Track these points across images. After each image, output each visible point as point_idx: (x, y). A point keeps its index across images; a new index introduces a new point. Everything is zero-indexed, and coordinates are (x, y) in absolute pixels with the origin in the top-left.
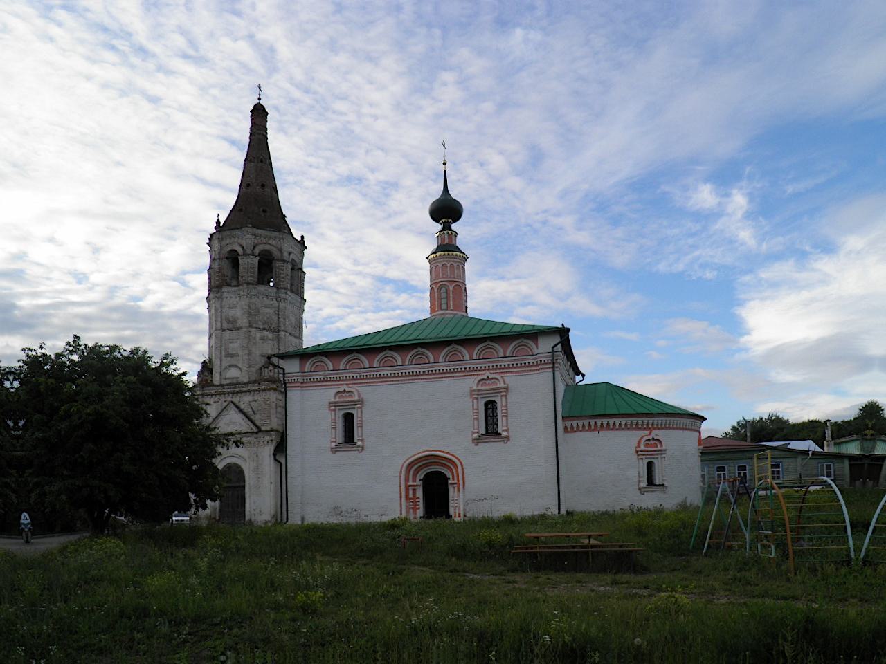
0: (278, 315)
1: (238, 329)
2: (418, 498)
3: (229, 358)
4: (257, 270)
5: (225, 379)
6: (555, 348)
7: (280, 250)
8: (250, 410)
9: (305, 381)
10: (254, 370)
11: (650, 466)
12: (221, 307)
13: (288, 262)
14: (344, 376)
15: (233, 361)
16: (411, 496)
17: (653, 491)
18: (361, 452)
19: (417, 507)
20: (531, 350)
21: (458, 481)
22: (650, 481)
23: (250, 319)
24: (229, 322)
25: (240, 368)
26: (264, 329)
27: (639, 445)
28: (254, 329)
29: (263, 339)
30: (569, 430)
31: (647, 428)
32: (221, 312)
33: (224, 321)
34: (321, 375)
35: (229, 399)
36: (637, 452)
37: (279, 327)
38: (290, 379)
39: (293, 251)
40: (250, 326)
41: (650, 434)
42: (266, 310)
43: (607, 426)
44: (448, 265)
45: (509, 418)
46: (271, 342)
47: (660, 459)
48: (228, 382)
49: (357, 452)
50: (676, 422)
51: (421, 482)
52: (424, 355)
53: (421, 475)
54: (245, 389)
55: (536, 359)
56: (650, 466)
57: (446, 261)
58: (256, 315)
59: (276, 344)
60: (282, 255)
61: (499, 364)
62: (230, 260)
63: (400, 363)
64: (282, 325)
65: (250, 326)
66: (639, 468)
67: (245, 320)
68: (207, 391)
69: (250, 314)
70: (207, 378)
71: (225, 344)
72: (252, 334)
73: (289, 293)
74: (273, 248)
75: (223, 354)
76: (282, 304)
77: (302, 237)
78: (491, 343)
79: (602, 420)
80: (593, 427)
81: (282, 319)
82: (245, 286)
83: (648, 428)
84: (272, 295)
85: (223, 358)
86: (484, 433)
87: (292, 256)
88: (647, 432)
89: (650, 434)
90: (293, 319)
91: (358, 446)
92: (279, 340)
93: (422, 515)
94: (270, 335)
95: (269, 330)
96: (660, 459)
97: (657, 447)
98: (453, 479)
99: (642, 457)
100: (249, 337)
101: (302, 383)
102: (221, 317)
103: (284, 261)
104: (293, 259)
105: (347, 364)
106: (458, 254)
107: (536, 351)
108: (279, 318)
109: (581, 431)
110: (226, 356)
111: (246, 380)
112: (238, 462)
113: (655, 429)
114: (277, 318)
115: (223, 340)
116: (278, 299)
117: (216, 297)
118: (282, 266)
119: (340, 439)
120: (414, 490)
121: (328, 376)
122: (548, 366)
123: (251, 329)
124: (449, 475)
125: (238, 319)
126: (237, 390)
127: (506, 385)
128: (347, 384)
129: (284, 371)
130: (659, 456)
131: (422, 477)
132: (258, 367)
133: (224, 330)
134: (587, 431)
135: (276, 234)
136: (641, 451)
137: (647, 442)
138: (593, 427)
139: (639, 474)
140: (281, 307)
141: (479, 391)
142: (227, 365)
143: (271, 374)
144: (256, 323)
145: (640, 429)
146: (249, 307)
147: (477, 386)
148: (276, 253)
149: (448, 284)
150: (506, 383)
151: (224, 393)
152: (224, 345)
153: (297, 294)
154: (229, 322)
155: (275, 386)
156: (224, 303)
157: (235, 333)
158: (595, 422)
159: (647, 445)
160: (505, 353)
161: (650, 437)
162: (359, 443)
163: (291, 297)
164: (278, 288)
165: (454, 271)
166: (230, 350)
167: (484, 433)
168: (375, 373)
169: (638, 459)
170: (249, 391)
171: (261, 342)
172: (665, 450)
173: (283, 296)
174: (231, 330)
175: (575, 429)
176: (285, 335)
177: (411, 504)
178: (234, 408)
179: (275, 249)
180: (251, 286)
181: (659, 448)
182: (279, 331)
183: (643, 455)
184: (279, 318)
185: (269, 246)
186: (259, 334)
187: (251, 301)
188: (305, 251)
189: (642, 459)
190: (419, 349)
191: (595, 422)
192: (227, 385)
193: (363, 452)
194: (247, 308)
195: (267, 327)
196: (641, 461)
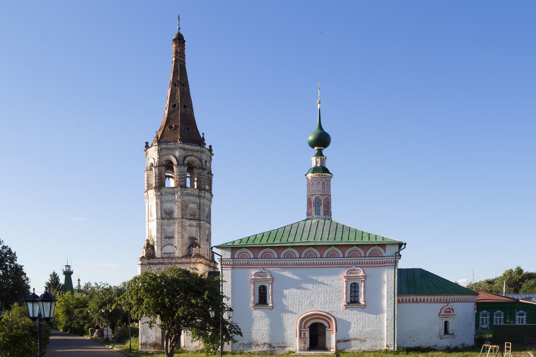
1: (174, 219)
2: (306, 338)
3: (167, 240)
5: (164, 254)
6: (396, 254)
7: (201, 160)
9: (235, 264)
10: (185, 248)
11: (446, 323)
12: (161, 202)
14: (261, 262)
16: (303, 336)
17: (447, 338)
18: (271, 310)
19: (306, 343)
20: (381, 254)
21: (333, 329)
22: (446, 332)
23: (183, 213)
24: (167, 213)
26: (191, 219)
27: (441, 312)
28: (185, 220)
29: (190, 226)
30: (401, 302)
31: (446, 302)
32: (161, 206)
34: (245, 261)
36: (439, 315)
37: (200, 218)
38: (225, 262)
40: (183, 218)
41: (447, 306)
42: (192, 206)
43: (423, 300)
44: (321, 183)
45: (366, 294)
46: (195, 229)
47: (452, 319)
48: (166, 256)
49: (269, 309)
50: (462, 298)
51: (309, 328)
52: (313, 252)
53: (309, 324)
54: (179, 261)
55: (384, 259)
56: (446, 323)
57: (320, 180)
58: (186, 210)
59: (198, 230)
60: (202, 164)
61: (361, 261)
62: (165, 166)
63: (298, 256)
64: (202, 216)
65: (183, 218)
66: (440, 325)
67: (180, 214)
68: (151, 261)
69: (182, 209)
70: (150, 252)
71: (164, 229)
72: (183, 224)
74: (196, 159)
75: (163, 236)
76: (202, 201)
77: (210, 146)
78: (357, 248)
79: (421, 297)
80: (415, 301)
81: (202, 212)
82: (179, 188)
83: (447, 302)
84: (196, 195)
85: (163, 239)
86: (350, 302)
88: (446, 304)
89: (447, 306)
90: (207, 209)
91: (269, 307)
92: (200, 227)
93: (308, 347)
94: (194, 223)
95: (194, 219)
96: (452, 319)
97: (451, 313)
98: (330, 328)
99: (442, 318)
100: (183, 226)
101: (232, 265)
102: (161, 210)
105: (263, 255)
106: (330, 175)
107: (384, 254)
109: (408, 303)
111: (180, 255)
113: (451, 302)
114: (198, 211)
116: (199, 197)
117: (157, 194)
119: (257, 301)
120: (304, 334)
121: (250, 262)
122: (392, 264)
124: (326, 324)
126: (174, 261)
127: (364, 275)
128: (262, 268)
129: (221, 257)
130: (452, 318)
131: (309, 326)
132: (187, 246)
134: (411, 303)
135: (198, 148)
136: (442, 315)
137: (446, 310)
138: (415, 301)
139: (440, 328)
140: (201, 203)
141: (348, 277)
143: (198, 252)
144: (186, 215)
145: (443, 303)
147: (347, 274)
148: (197, 162)
149: (321, 197)
150: (365, 273)
151: (164, 264)
152: (163, 230)
154: (167, 213)
155: (201, 261)
156: (163, 200)
157: (171, 221)
158: (417, 298)
159: (445, 312)
160: (365, 254)
161: (447, 307)
162: (271, 305)
163: (207, 195)
164: (200, 190)
165: (325, 188)
166: (167, 234)
167: (350, 302)
168: (281, 262)
169: (440, 320)
171: (189, 228)
172: (456, 315)
173: (202, 194)
174: (168, 219)
175: (404, 301)
176: (204, 224)
177: (303, 341)
179: (198, 160)
180: (183, 189)
181: (452, 313)
183: (443, 317)
184: (200, 211)
185: (194, 158)
186: (188, 222)
187: (183, 199)
189: (442, 319)
190: (311, 248)
191: (417, 298)
192: (166, 258)
193: (273, 310)
194: (180, 204)
195: (192, 217)
196: (441, 321)
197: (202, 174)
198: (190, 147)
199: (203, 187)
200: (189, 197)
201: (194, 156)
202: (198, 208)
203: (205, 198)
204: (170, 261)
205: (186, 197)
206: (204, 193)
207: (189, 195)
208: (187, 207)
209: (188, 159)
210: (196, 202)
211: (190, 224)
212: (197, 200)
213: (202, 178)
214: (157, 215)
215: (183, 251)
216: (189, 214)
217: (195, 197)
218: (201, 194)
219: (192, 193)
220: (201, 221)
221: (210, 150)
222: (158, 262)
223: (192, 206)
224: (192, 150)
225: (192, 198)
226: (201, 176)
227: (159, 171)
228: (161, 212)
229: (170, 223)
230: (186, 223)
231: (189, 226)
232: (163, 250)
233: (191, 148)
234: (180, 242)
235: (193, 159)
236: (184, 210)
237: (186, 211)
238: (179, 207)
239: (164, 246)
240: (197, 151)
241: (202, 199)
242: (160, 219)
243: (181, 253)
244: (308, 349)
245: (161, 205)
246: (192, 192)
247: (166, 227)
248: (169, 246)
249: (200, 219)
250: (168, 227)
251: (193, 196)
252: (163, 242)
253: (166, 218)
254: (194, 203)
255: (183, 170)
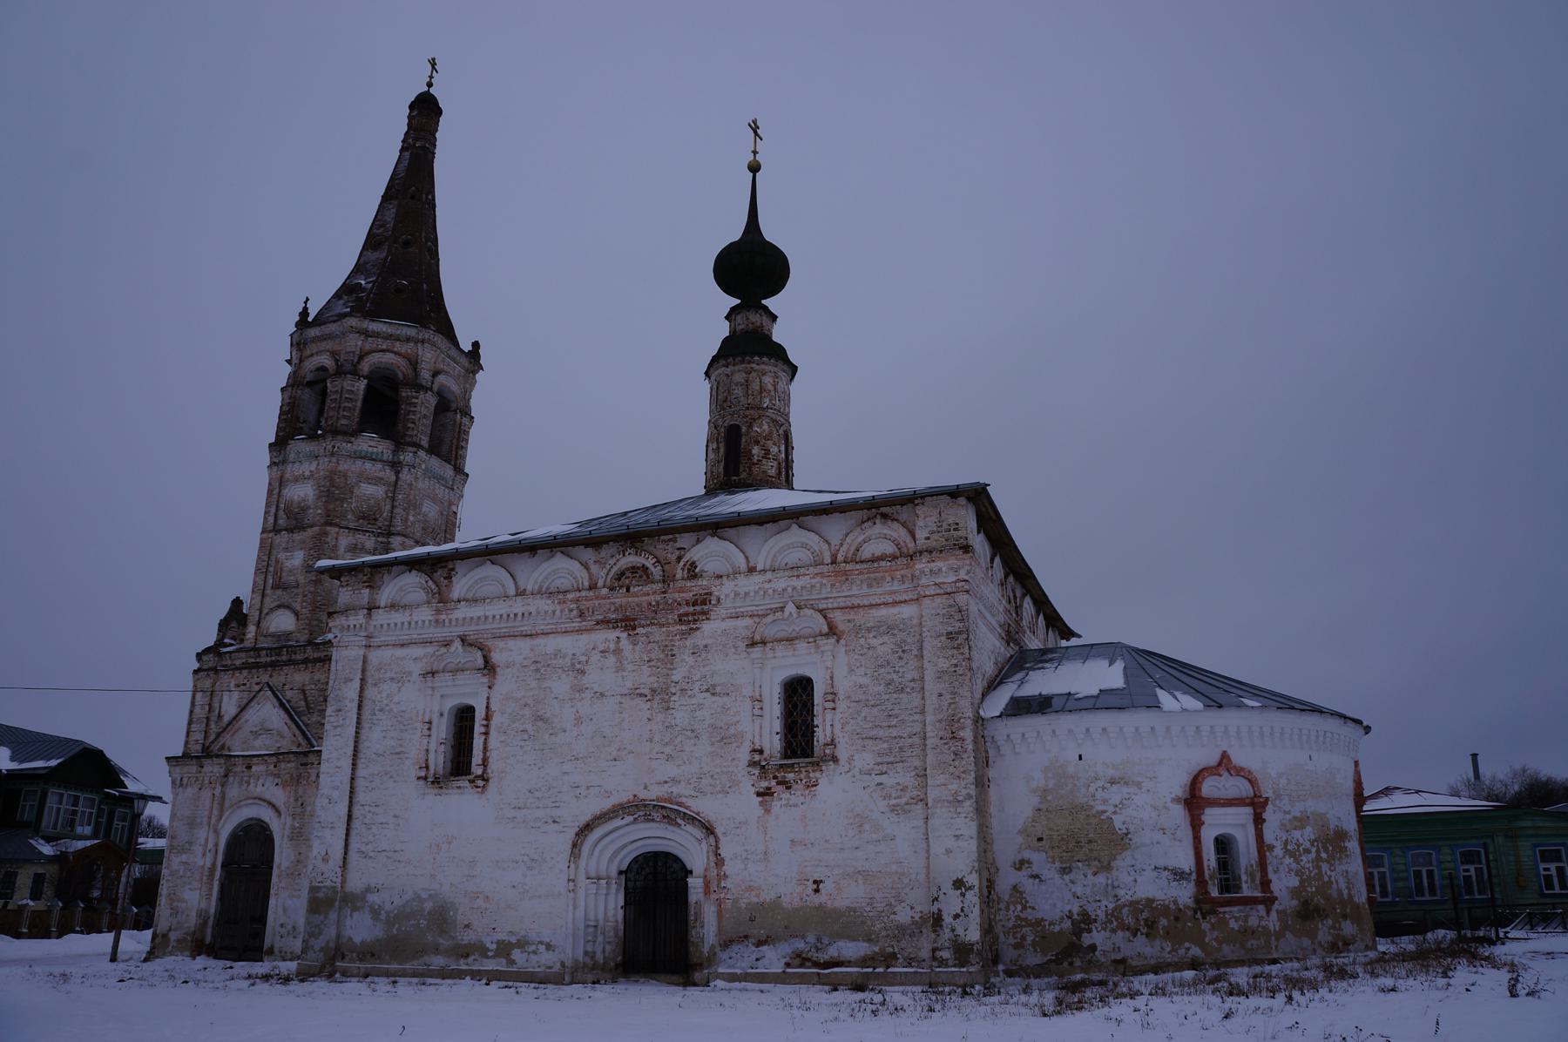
0: (393, 499)
3: (279, 592)
4: (359, 404)
7: (414, 363)
8: (303, 703)
12: (280, 484)
13: (426, 389)
15: (286, 599)
23: (331, 506)
25: (296, 614)
33: (281, 513)
35: (265, 678)
39: (446, 368)
42: (368, 490)
58: (343, 500)
64: (398, 522)
73: (422, 454)
84: (385, 458)
85: (268, 591)
87: (441, 378)
102: (277, 506)
103: (419, 387)
104: (442, 386)
108: (393, 507)
110: (275, 587)
112: (266, 815)
114: (388, 507)
115: (274, 552)
116: (396, 466)
118: (413, 397)
123: (328, 528)
125: (309, 507)
133: (276, 530)
142: (276, 604)
146: (331, 480)
151: (257, 666)
153: (448, 461)
156: (287, 476)
166: (284, 574)
170: (306, 661)
174: (290, 530)
178: (272, 697)
182: (390, 534)
184: (393, 507)
188: (480, 376)
197: (414, 400)
198: (384, 330)
199: (411, 436)
200: (359, 462)
201: (396, 353)
202: (388, 497)
203: (414, 468)
204: (273, 658)
205: (349, 462)
206: (411, 454)
207: (361, 458)
208: (352, 492)
209: (375, 358)
210: (382, 479)
211: (354, 542)
212: (389, 475)
213: (410, 411)
214: (265, 518)
215: (315, 623)
216: (354, 513)
217: (379, 466)
218: (402, 457)
219: (372, 453)
220: (393, 534)
221: (475, 352)
222: (244, 661)
223: (368, 490)
224: (389, 337)
225: (368, 465)
226: (408, 407)
227: (290, 399)
228: (277, 510)
229: (293, 541)
230: (340, 538)
231: (348, 551)
232: (264, 624)
233: (389, 331)
234: (309, 595)
235: (391, 361)
236: (337, 500)
237: (345, 505)
238: (323, 491)
239: (267, 614)
240: (408, 340)
241: (405, 470)
242: (270, 532)
243: (306, 631)
244: (621, 969)
245: (280, 491)
246: (370, 449)
247: (282, 556)
248: (281, 611)
249: (392, 529)
250: (289, 554)
251: (373, 460)
252: (267, 600)
253: (286, 530)
254: (377, 481)
255: (349, 388)
